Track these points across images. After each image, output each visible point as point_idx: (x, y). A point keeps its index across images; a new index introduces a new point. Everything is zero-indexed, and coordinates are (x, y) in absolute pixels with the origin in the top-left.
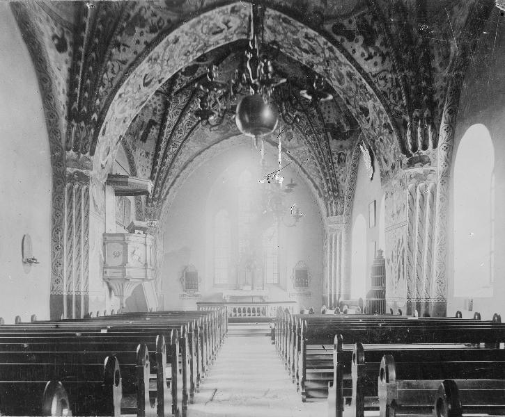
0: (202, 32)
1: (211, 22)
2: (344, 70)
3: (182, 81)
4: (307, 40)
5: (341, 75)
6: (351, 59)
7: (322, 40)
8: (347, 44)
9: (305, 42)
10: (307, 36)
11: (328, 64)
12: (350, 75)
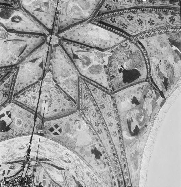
0: (13, 147)
1: (19, 143)
2: (85, 171)
4: (66, 156)
5: (83, 174)
6: (88, 165)
7: (74, 155)
8: (86, 158)
9: (66, 157)
10: (67, 154)
11: (77, 168)
12: (88, 174)
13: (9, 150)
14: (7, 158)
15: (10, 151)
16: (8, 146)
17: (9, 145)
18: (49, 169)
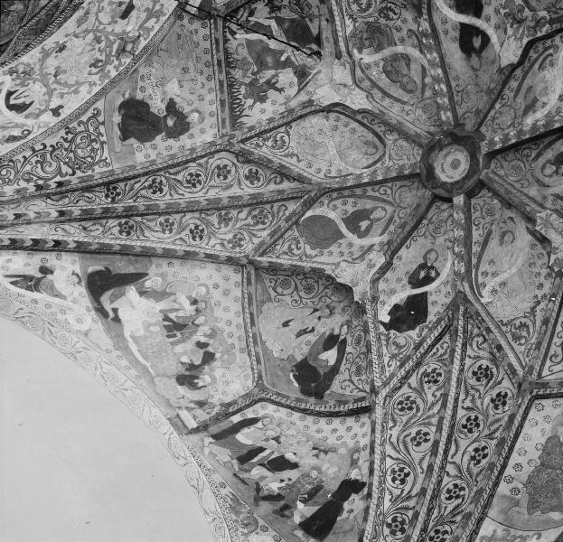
0: (100, 23)
3: (398, 346)
13: (98, 40)
14: (116, 63)
15: (103, 38)
16: (87, 31)
17: (84, 26)
18: (526, 113)
